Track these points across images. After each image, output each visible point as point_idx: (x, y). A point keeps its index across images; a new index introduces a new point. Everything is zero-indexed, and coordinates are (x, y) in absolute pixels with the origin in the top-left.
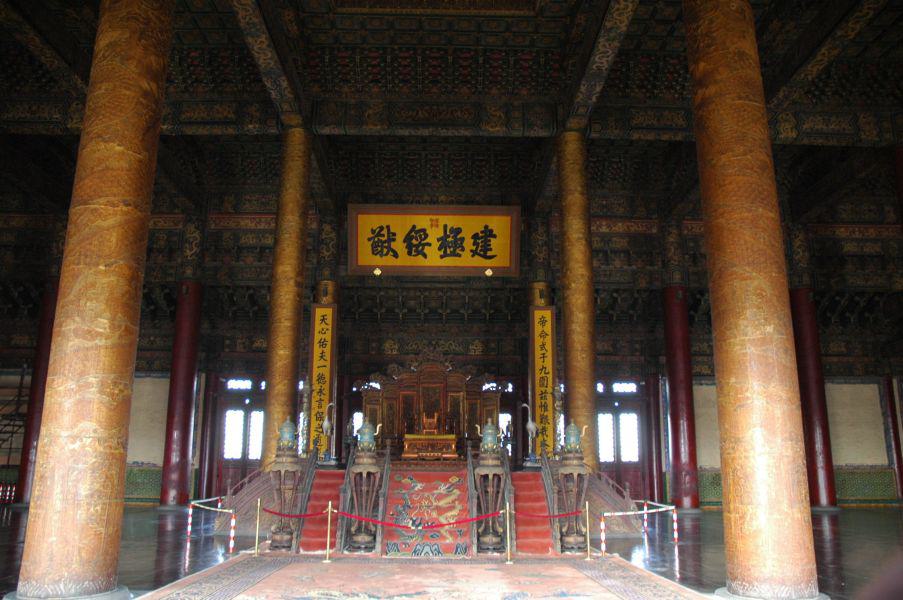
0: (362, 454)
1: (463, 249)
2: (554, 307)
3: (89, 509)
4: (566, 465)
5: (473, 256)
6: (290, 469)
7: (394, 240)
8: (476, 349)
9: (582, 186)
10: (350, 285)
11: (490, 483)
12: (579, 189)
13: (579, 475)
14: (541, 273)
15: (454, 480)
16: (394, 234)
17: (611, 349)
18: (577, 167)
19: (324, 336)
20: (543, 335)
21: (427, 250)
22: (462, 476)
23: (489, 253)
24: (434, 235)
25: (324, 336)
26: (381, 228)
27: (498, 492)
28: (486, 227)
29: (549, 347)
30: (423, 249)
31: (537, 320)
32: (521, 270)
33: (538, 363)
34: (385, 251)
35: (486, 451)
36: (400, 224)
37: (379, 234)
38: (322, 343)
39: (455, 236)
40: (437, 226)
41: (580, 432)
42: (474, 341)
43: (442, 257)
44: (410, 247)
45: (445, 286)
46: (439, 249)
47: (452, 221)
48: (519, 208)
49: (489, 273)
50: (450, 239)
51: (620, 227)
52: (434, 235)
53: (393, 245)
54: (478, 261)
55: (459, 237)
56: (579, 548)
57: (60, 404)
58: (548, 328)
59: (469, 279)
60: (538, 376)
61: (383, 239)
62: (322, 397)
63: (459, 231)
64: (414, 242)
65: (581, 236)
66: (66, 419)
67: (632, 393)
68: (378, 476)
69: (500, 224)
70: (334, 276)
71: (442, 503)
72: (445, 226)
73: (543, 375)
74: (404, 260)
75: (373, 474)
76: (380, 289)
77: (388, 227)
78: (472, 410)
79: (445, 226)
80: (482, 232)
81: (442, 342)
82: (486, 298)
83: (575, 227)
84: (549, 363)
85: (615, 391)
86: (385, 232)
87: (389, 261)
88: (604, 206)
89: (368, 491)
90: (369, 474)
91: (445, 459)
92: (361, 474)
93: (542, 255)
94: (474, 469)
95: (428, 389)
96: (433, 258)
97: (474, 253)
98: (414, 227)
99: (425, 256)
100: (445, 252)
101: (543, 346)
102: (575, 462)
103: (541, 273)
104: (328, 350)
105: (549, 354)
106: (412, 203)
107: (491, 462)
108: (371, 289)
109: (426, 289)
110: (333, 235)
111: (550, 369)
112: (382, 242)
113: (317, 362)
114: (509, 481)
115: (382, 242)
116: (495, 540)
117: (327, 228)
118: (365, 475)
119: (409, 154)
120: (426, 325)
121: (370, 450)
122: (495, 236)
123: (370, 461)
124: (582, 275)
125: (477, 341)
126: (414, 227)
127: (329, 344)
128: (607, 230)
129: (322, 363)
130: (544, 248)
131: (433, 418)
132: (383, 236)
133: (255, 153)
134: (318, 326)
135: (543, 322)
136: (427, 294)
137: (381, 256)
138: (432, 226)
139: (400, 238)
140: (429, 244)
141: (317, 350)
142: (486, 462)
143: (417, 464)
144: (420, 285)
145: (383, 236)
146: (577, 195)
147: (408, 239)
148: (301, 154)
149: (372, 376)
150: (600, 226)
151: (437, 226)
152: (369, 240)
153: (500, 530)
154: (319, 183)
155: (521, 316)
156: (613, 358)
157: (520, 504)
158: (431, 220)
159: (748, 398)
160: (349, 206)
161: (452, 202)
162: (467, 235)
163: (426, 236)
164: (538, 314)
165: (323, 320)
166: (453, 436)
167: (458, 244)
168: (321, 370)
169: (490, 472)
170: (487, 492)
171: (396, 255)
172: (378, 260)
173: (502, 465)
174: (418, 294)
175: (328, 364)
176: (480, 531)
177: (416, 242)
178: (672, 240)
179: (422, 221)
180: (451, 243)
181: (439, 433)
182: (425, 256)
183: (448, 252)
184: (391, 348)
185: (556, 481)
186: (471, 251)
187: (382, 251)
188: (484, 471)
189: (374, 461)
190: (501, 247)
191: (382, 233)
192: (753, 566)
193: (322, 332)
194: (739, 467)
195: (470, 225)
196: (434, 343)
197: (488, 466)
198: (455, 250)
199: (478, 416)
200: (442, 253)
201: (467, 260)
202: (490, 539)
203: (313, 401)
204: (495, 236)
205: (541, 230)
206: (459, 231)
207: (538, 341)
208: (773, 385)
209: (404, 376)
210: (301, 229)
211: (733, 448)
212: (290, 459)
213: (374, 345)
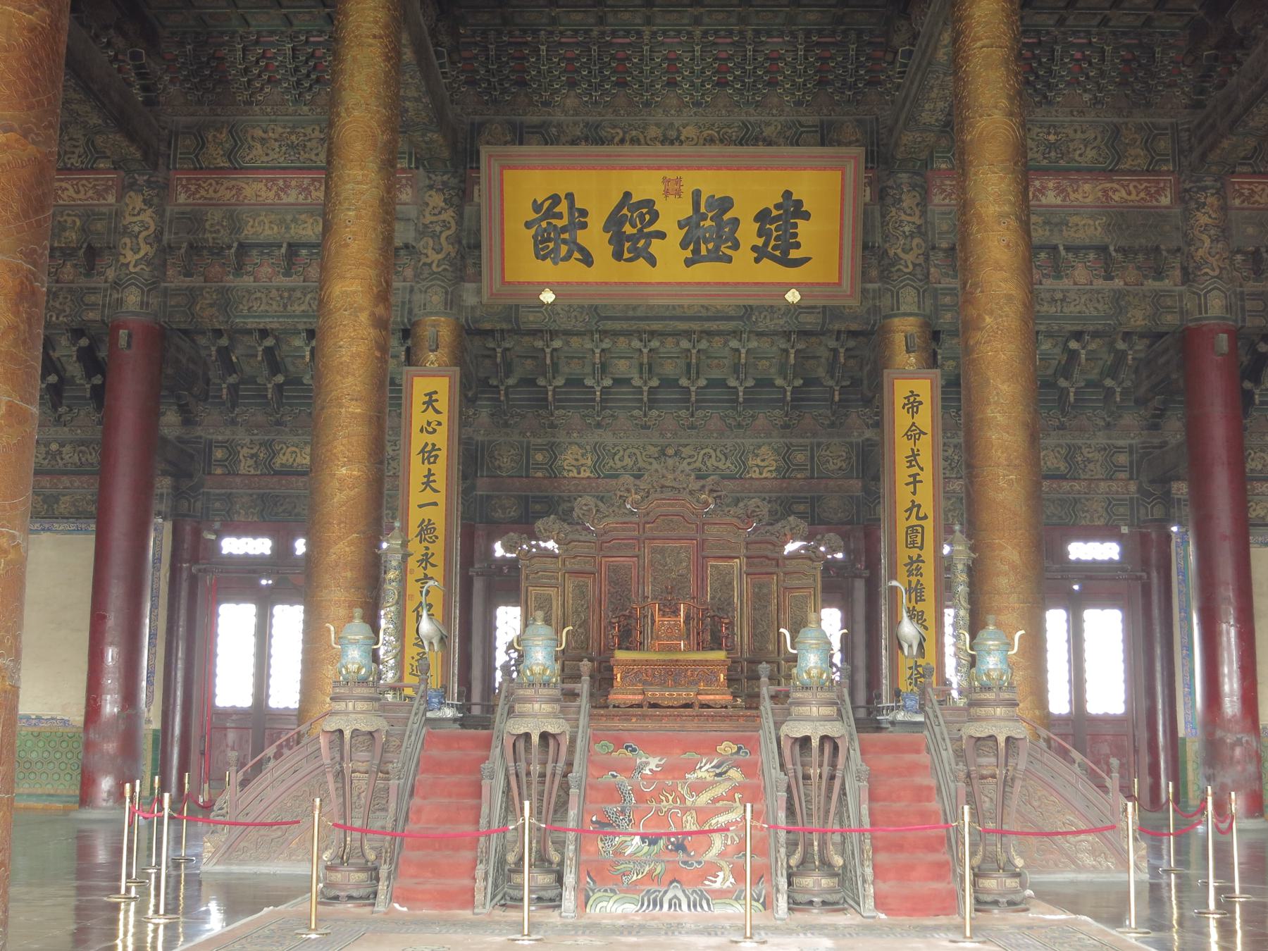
0: (530, 692)
1: (736, 246)
2: (938, 371)
4: (979, 719)
5: (757, 260)
7: (584, 226)
8: (764, 466)
9: (1011, 99)
10: (488, 326)
12: (1004, 103)
13: (1008, 739)
14: (909, 299)
15: (727, 748)
16: (584, 213)
17: (1063, 466)
18: (999, 54)
19: (430, 439)
20: (914, 433)
21: (656, 247)
22: (748, 744)
23: (794, 254)
24: (672, 213)
25: (430, 439)
26: (555, 199)
27: (832, 777)
28: (787, 194)
29: (925, 459)
30: (648, 245)
31: (899, 401)
32: (864, 291)
33: (903, 495)
34: (564, 249)
35: (806, 688)
36: (596, 187)
37: (551, 214)
38: (429, 454)
39: (717, 218)
40: (678, 193)
42: (760, 447)
43: (689, 263)
44: (618, 240)
45: (695, 326)
46: (684, 245)
47: (711, 183)
48: (859, 151)
49: (793, 296)
50: (708, 223)
51: (1087, 192)
52: (672, 213)
53: (582, 237)
54: (770, 271)
55: (726, 217)
56: (1011, 903)
58: (924, 419)
59: (749, 310)
60: (902, 526)
61: (559, 223)
62: (430, 571)
63: (725, 204)
64: (628, 229)
65: (1006, 208)
67: (1111, 561)
69: (821, 187)
70: (452, 302)
71: (704, 799)
72: (697, 194)
73: (913, 521)
74: (606, 270)
75: (554, 736)
76: (553, 334)
77: (570, 197)
78: (760, 599)
79: (697, 194)
80: (777, 207)
81: (686, 451)
82: (786, 351)
83: (992, 188)
84: (925, 495)
85: (1072, 557)
86: (563, 207)
87: (573, 271)
88: (1051, 146)
89: (543, 775)
90: (544, 736)
91: (703, 706)
92: (527, 736)
93: (909, 258)
94: (778, 725)
95: (662, 551)
96: (668, 268)
97: (760, 253)
98: (627, 195)
99: (652, 261)
100: (696, 251)
101: (913, 458)
102: (999, 711)
103: (909, 299)
104: (440, 469)
105: (927, 476)
106: (622, 141)
108: (534, 333)
109: (653, 334)
110: (448, 215)
111: (927, 508)
112: (556, 229)
113: (417, 495)
114: (856, 755)
115: (556, 229)
116: (825, 882)
117: (437, 200)
118: (535, 739)
119: (613, 33)
120: (655, 413)
121: (546, 684)
122: (806, 216)
123: (546, 708)
124: (1009, 298)
125: (763, 449)
126: (627, 195)
127: (443, 455)
128: (1059, 201)
129: (429, 496)
130: (916, 241)
131: (676, 612)
132: (560, 216)
133: (272, 33)
134: (419, 416)
135: (913, 404)
136: (655, 344)
137: (556, 263)
138: (667, 193)
139: (596, 221)
140: (662, 235)
141: (417, 470)
143: (644, 717)
144: (643, 325)
145: (560, 216)
146: (998, 116)
147: (614, 222)
148: (376, 31)
149: (539, 525)
150: (1042, 190)
151: (678, 193)
152: (528, 225)
153: (838, 861)
154: (418, 100)
155: (865, 390)
156: (1066, 485)
157: (877, 805)
158: (666, 181)
160: (484, 151)
161: (710, 141)
162: (745, 212)
163: (655, 216)
164: (901, 389)
165: (430, 402)
166: (720, 655)
167: (726, 234)
168: (429, 513)
169: (814, 731)
170: (806, 777)
171: (587, 260)
172: (546, 270)
174: (636, 344)
175: (441, 498)
176: (794, 861)
177: (631, 229)
178: (1204, 220)
179: (646, 184)
180: (709, 232)
181: (689, 649)
182: (652, 261)
183: (704, 252)
184: (575, 462)
185: (960, 755)
186: (754, 248)
187: (556, 249)
189: (557, 707)
190: (821, 237)
191: (557, 210)
193: (428, 429)
195: (752, 188)
196: (670, 451)
198: (717, 248)
199: (774, 607)
200: (688, 253)
201: (745, 270)
202: (814, 882)
203: (410, 579)
204: (806, 216)
205: (908, 201)
206: (725, 204)
207: (902, 448)
209: (610, 522)
210: (382, 200)
212: (361, 706)
213: (539, 457)
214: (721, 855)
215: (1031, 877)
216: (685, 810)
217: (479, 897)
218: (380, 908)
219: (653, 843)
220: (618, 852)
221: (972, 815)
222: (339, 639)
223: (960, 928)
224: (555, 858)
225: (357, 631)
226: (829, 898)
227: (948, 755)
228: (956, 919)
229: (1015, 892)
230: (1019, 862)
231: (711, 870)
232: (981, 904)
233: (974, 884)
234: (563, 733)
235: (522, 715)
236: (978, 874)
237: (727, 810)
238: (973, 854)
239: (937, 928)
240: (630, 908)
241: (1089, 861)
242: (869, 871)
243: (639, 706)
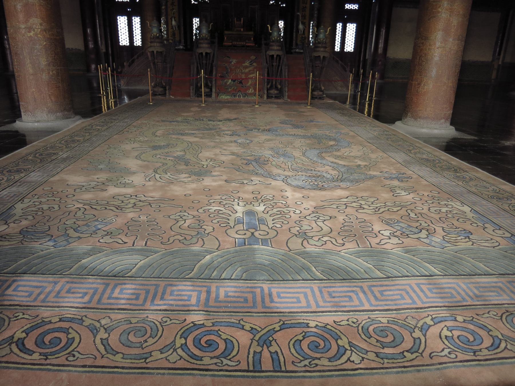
0: (202, 41)
3: (49, 73)
4: (317, 51)
6: (159, 50)
11: (275, 59)
13: (324, 57)
15: (253, 57)
27: (279, 66)
35: (273, 41)
41: (326, 31)
56: (320, 98)
57: (15, 6)
66: (21, 16)
68: (212, 55)
71: (247, 70)
75: (209, 53)
89: (206, 64)
90: (206, 53)
92: (202, 53)
94: (266, 52)
102: (322, 49)
107: (275, 48)
116: (276, 92)
118: (204, 54)
121: (206, 39)
142: (273, 48)
153: (279, 87)
159: (439, 12)
166: (252, 33)
170: (273, 65)
173: (282, 50)
176: (268, 87)
188: (271, 53)
192: (419, 110)
194: (424, 55)
197: (273, 50)
202: (274, 92)
208: (456, 4)
211: (423, 43)
212: (158, 44)
214: (251, 84)
215: (325, 92)
216: (242, 73)
217: (191, 94)
218: (167, 97)
219: (234, 81)
220: (226, 83)
221: (313, 76)
222: (150, 25)
223: (307, 103)
224: (210, 85)
225: (155, 24)
226: (277, 96)
227: (308, 60)
228: (307, 101)
229: (321, 95)
230: (323, 88)
231: (249, 88)
232: (313, 98)
233: (312, 93)
234: (211, 53)
235: (200, 47)
236: (313, 90)
237: (253, 73)
238: (312, 86)
239: (301, 103)
240: (228, 97)
241: (340, 89)
242: (286, 89)
243: (231, 46)
